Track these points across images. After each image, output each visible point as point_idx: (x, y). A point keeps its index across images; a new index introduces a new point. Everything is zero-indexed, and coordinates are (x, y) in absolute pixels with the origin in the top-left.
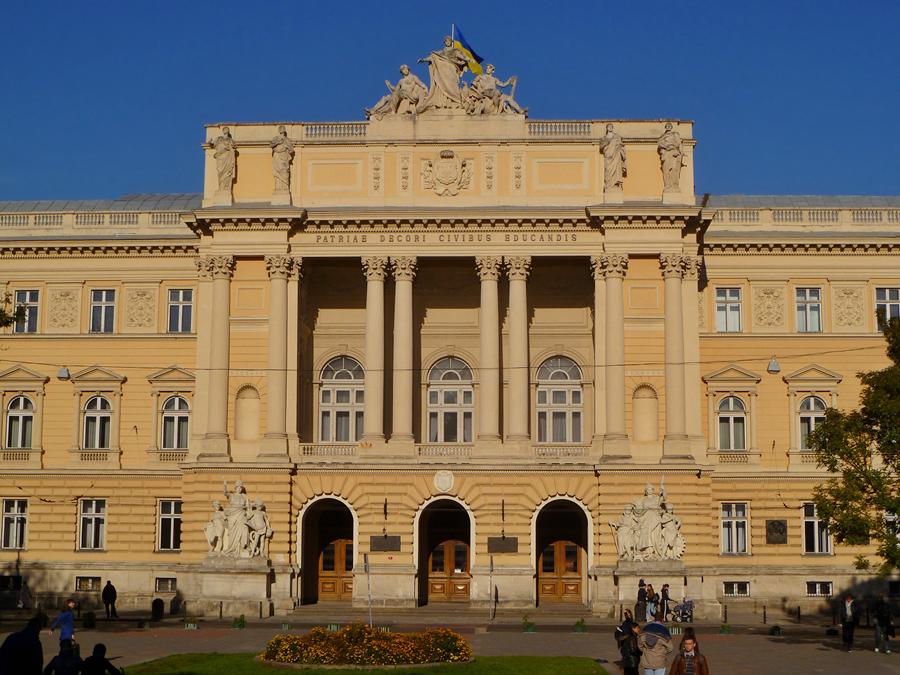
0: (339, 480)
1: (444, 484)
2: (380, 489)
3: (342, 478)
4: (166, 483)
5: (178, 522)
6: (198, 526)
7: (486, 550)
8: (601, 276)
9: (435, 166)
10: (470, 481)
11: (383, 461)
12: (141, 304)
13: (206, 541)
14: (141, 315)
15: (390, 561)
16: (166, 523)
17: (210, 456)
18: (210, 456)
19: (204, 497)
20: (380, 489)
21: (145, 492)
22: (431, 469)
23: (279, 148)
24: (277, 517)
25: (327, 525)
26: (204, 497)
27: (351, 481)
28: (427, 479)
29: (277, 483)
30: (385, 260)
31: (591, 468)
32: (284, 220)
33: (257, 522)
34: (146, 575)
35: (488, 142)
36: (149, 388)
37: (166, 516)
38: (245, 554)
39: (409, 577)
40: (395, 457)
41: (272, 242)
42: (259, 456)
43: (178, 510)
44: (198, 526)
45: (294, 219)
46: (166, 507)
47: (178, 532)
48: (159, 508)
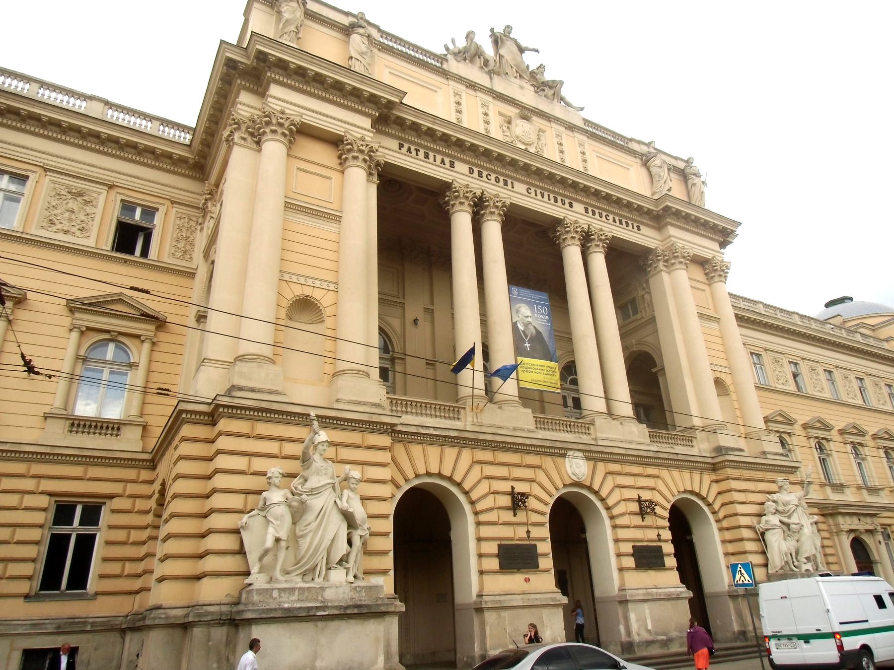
0: (451, 453)
1: (577, 467)
2: (503, 471)
3: (456, 450)
4: (77, 471)
6: (218, 521)
7: (634, 565)
8: (664, 268)
9: (513, 123)
10: (601, 467)
11: (500, 432)
12: (72, 204)
14: (70, 220)
15: (526, 587)
16: (58, 544)
17: (253, 390)
18: (253, 390)
20: (503, 471)
21: (29, 484)
22: (558, 452)
23: (361, 31)
25: (423, 528)
27: (466, 456)
28: (559, 460)
30: (478, 193)
31: (710, 460)
32: (373, 100)
35: (558, 120)
36: (67, 321)
37: (62, 530)
38: (338, 576)
39: (554, 610)
40: (515, 429)
41: (355, 125)
44: (218, 521)
45: (390, 105)
46: (63, 513)
48: (51, 515)
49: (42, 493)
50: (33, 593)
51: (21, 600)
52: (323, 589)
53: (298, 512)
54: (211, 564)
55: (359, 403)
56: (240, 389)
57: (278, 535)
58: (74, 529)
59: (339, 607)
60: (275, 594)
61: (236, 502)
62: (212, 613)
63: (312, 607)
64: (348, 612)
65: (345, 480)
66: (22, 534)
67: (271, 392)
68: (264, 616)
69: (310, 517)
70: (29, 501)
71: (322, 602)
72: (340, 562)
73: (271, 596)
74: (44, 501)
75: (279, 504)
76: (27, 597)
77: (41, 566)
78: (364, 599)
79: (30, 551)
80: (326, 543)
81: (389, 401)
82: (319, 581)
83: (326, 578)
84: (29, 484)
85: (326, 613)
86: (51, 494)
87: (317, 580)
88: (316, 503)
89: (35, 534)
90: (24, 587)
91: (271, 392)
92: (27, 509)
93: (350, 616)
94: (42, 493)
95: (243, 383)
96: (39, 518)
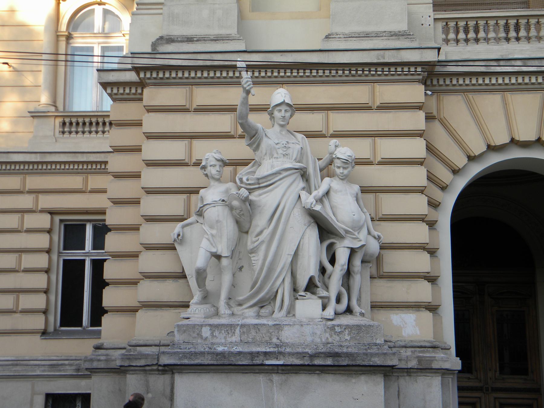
4: (75, 182)
5: (98, 265)
13: (183, 276)
16: (72, 271)
17: (189, 40)
18: (189, 40)
19: (174, 150)
21: (26, 201)
24: (392, 204)
26: (174, 150)
29: (385, 107)
33: (345, 207)
34: (25, 386)
37: (74, 255)
38: (309, 307)
42: (327, 37)
43: (99, 244)
46: (73, 234)
47: (100, 284)
48: (58, 237)
49: (42, 211)
50: (51, 329)
51: (38, 337)
52: (278, 327)
53: (243, 216)
54: (149, 291)
55: (367, 36)
56: (170, 40)
57: (214, 250)
58: (88, 254)
59: (302, 355)
60: (206, 332)
61: (173, 205)
62: (146, 356)
63: (258, 353)
64: (317, 362)
65: (331, 162)
66: (29, 261)
67: (217, 39)
68: (186, 361)
69: (260, 221)
70: (31, 221)
71: (277, 346)
72: (311, 287)
73: (200, 335)
74: (44, 221)
75: (214, 204)
76: (44, 333)
77: (56, 298)
78: (347, 343)
79: (40, 281)
80: (286, 259)
81: (440, 25)
82: (279, 315)
83: (291, 311)
84: (26, 201)
85: (281, 362)
86: (52, 213)
87: (277, 315)
88: (267, 200)
89: (42, 261)
90: (38, 322)
91: (217, 39)
92: (29, 231)
93: (323, 369)
94: (42, 211)
95: (177, 31)
96: (43, 241)
